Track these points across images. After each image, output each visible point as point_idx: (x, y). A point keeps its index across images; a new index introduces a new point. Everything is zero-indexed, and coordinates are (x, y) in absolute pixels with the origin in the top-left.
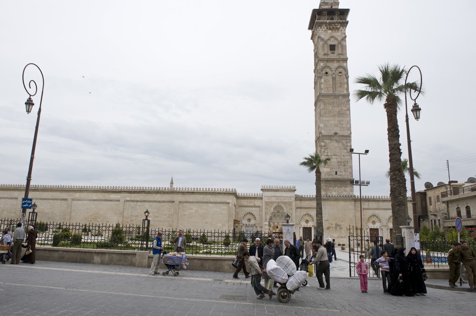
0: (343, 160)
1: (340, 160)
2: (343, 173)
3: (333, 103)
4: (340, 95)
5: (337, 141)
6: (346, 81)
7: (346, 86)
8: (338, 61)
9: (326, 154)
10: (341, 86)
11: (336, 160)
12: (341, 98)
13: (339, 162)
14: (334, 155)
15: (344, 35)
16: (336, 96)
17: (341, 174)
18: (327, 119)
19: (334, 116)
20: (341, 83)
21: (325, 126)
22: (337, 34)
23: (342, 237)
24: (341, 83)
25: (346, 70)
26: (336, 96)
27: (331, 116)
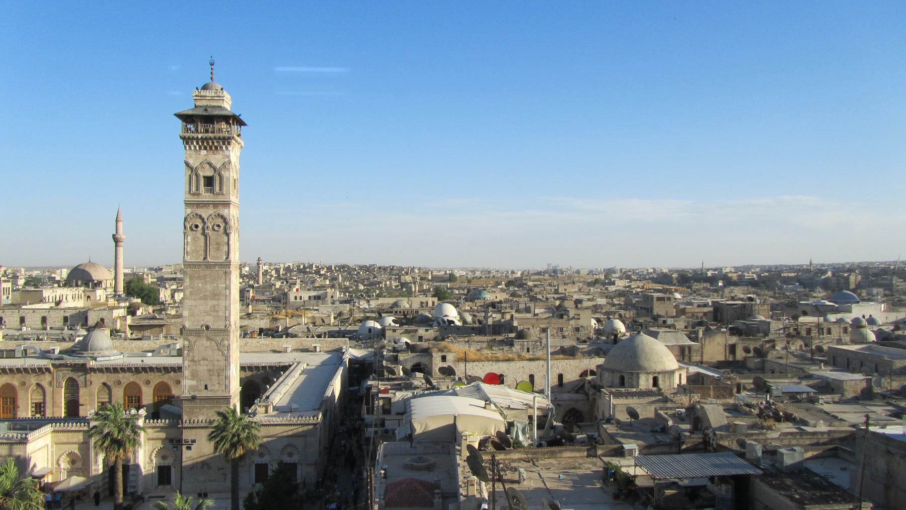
0: (216, 368)
1: (211, 367)
2: (217, 387)
3: (205, 276)
4: (216, 265)
5: (209, 339)
6: (226, 239)
7: (226, 248)
8: (216, 205)
9: (190, 358)
10: (218, 249)
11: (205, 368)
12: (217, 268)
13: (210, 371)
14: (204, 359)
15: (227, 160)
16: (209, 266)
17: (213, 388)
18: (193, 303)
19: (205, 298)
20: (218, 244)
21: (192, 315)
22: (217, 156)
23: (210, 481)
24: (218, 244)
25: (226, 221)
26: (209, 266)
27: (200, 299)
